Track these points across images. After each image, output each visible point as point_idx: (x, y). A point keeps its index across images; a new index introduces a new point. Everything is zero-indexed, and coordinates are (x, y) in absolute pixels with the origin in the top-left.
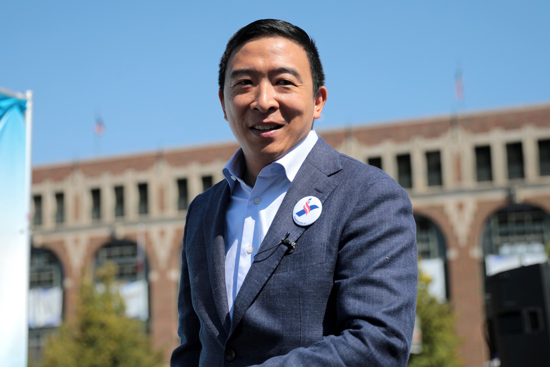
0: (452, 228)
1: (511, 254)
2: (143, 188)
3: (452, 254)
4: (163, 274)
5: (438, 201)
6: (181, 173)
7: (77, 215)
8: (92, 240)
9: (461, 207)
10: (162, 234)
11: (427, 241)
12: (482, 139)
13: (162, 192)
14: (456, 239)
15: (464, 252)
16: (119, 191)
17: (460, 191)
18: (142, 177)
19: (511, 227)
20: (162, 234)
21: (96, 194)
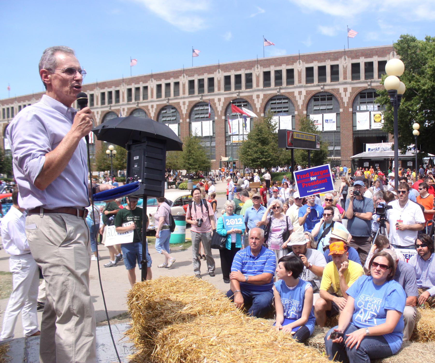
0: (342, 99)
1: (367, 111)
2: (211, 80)
3: (341, 110)
4: (220, 117)
5: (336, 87)
6: (227, 74)
7: (184, 93)
8: (190, 102)
9: (345, 90)
10: (219, 100)
11: (331, 105)
12: (355, 61)
13: (219, 82)
14: (343, 103)
15: (346, 109)
16: (201, 82)
17: (345, 83)
18: (211, 76)
19: (367, 100)
20: (219, 100)
21: (191, 83)
